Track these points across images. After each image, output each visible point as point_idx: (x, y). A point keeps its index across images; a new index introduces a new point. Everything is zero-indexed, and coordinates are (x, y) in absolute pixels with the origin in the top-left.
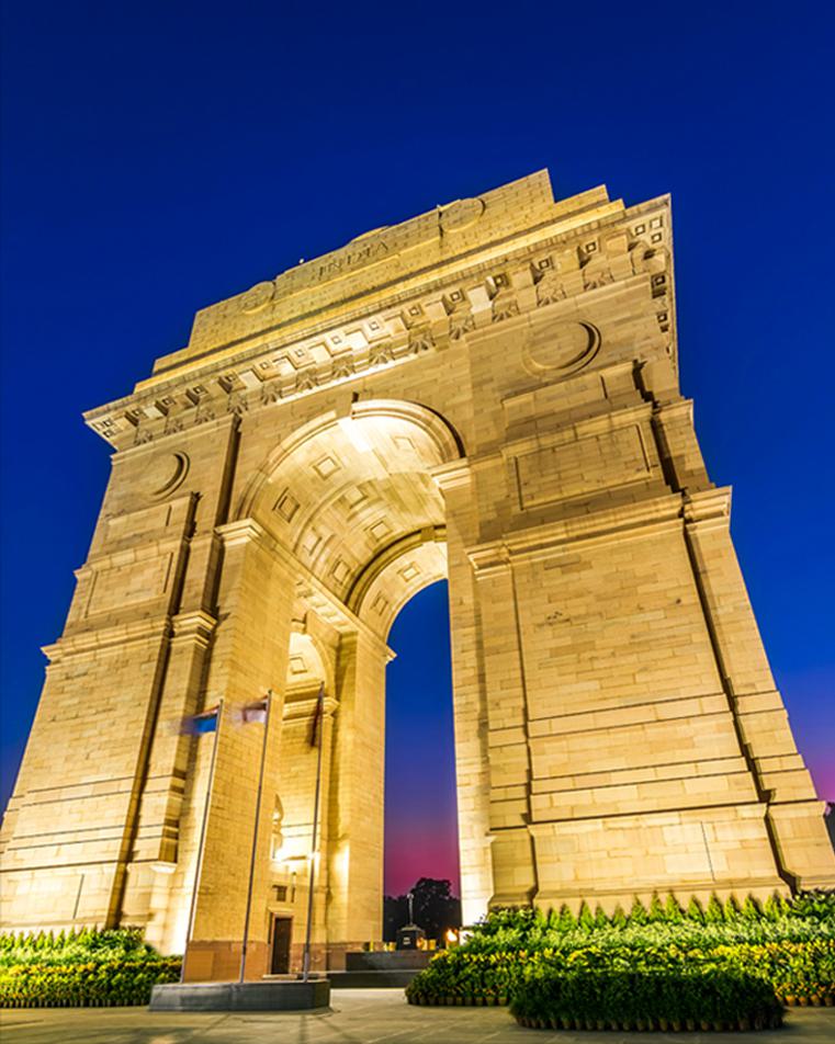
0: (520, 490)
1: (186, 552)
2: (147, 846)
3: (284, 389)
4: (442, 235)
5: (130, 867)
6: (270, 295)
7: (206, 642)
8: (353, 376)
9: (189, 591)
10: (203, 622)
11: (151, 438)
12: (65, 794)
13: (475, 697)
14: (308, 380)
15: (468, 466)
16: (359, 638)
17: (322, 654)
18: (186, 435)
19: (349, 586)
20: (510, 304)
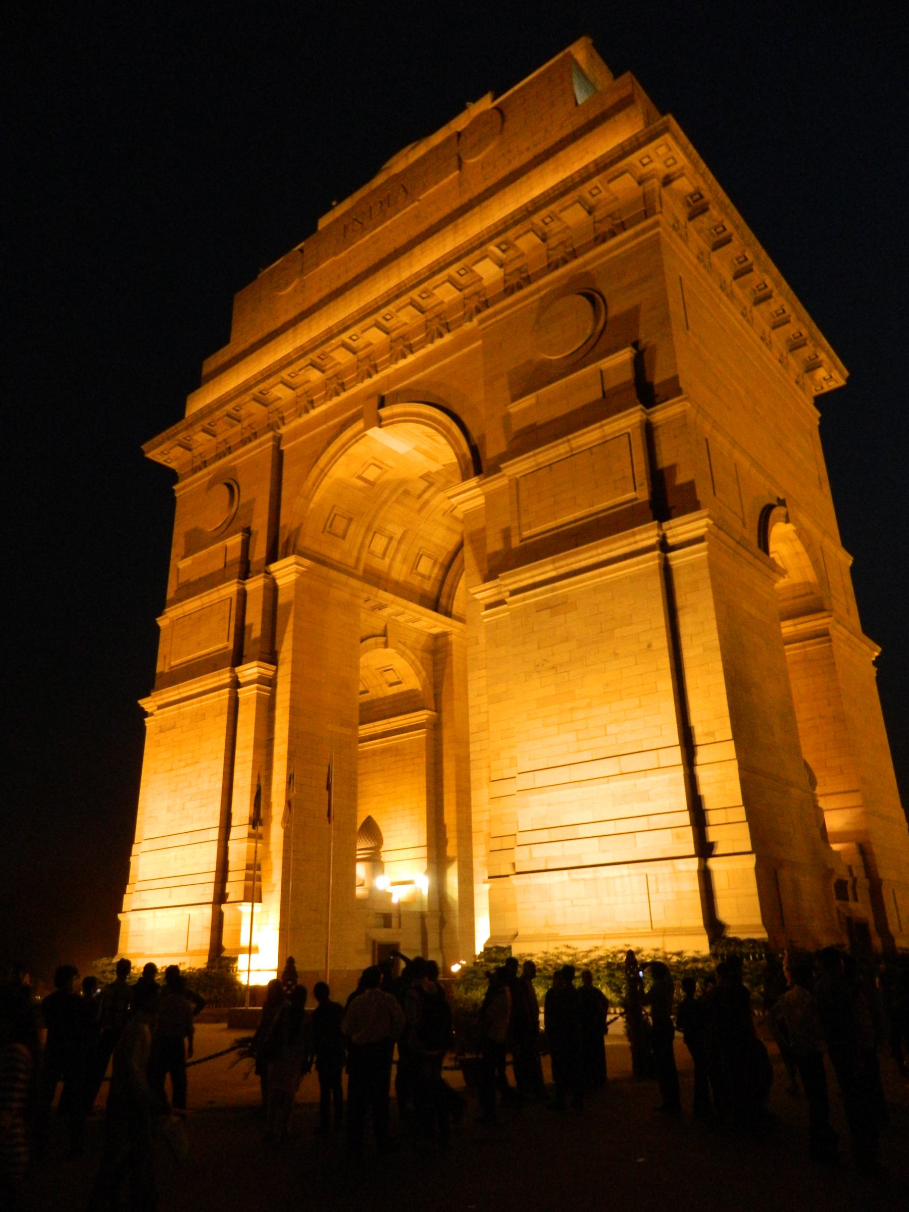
0: (519, 518)
1: (243, 595)
2: (234, 889)
3: (315, 398)
4: (460, 167)
7: (269, 688)
8: (376, 377)
10: (262, 670)
11: (205, 464)
15: (479, 486)
16: (453, 638)
17: (412, 664)
18: (235, 459)
19: (440, 578)
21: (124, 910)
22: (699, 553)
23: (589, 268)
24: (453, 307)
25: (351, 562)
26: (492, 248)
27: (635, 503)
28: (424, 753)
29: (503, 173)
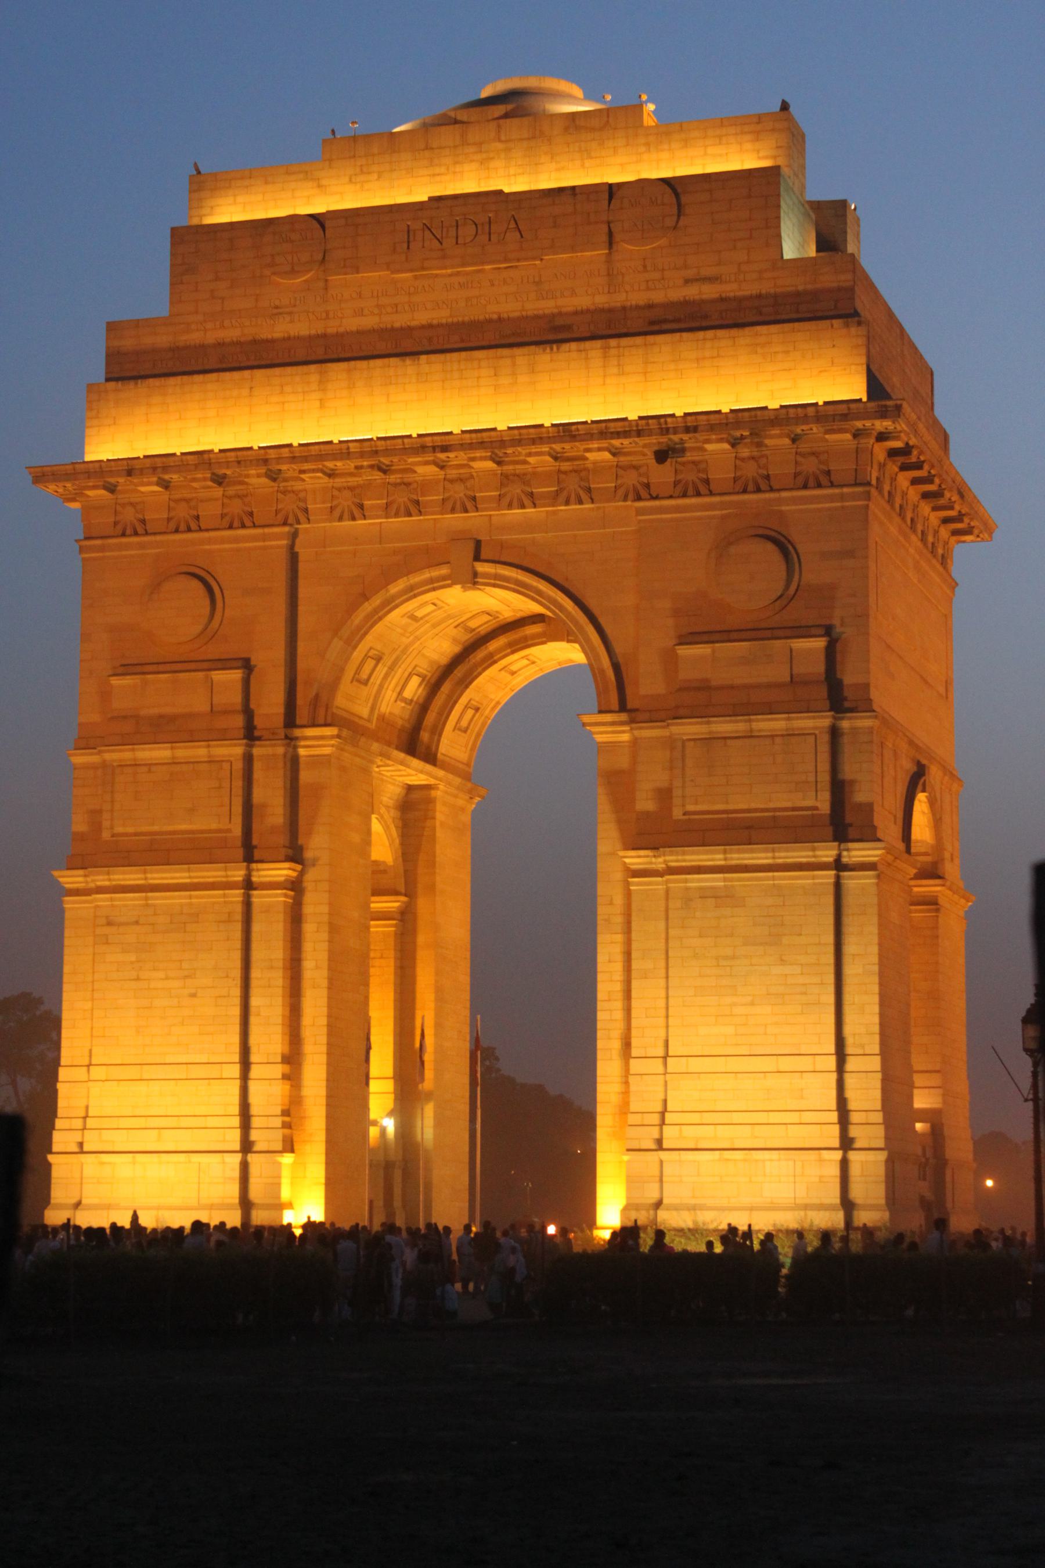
2: (266, 1133)
4: (610, 244)
5: (250, 1157)
6: (320, 257)
7: (292, 893)
12: (148, 1072)
13: (619, 1015)
14: (406, 499)
18: (210, 541)
21: (55, 1149)
23: (783, 508)
24: (599, 468)
25: (365, 712)
27: (815, 812)
28: (391, 954)
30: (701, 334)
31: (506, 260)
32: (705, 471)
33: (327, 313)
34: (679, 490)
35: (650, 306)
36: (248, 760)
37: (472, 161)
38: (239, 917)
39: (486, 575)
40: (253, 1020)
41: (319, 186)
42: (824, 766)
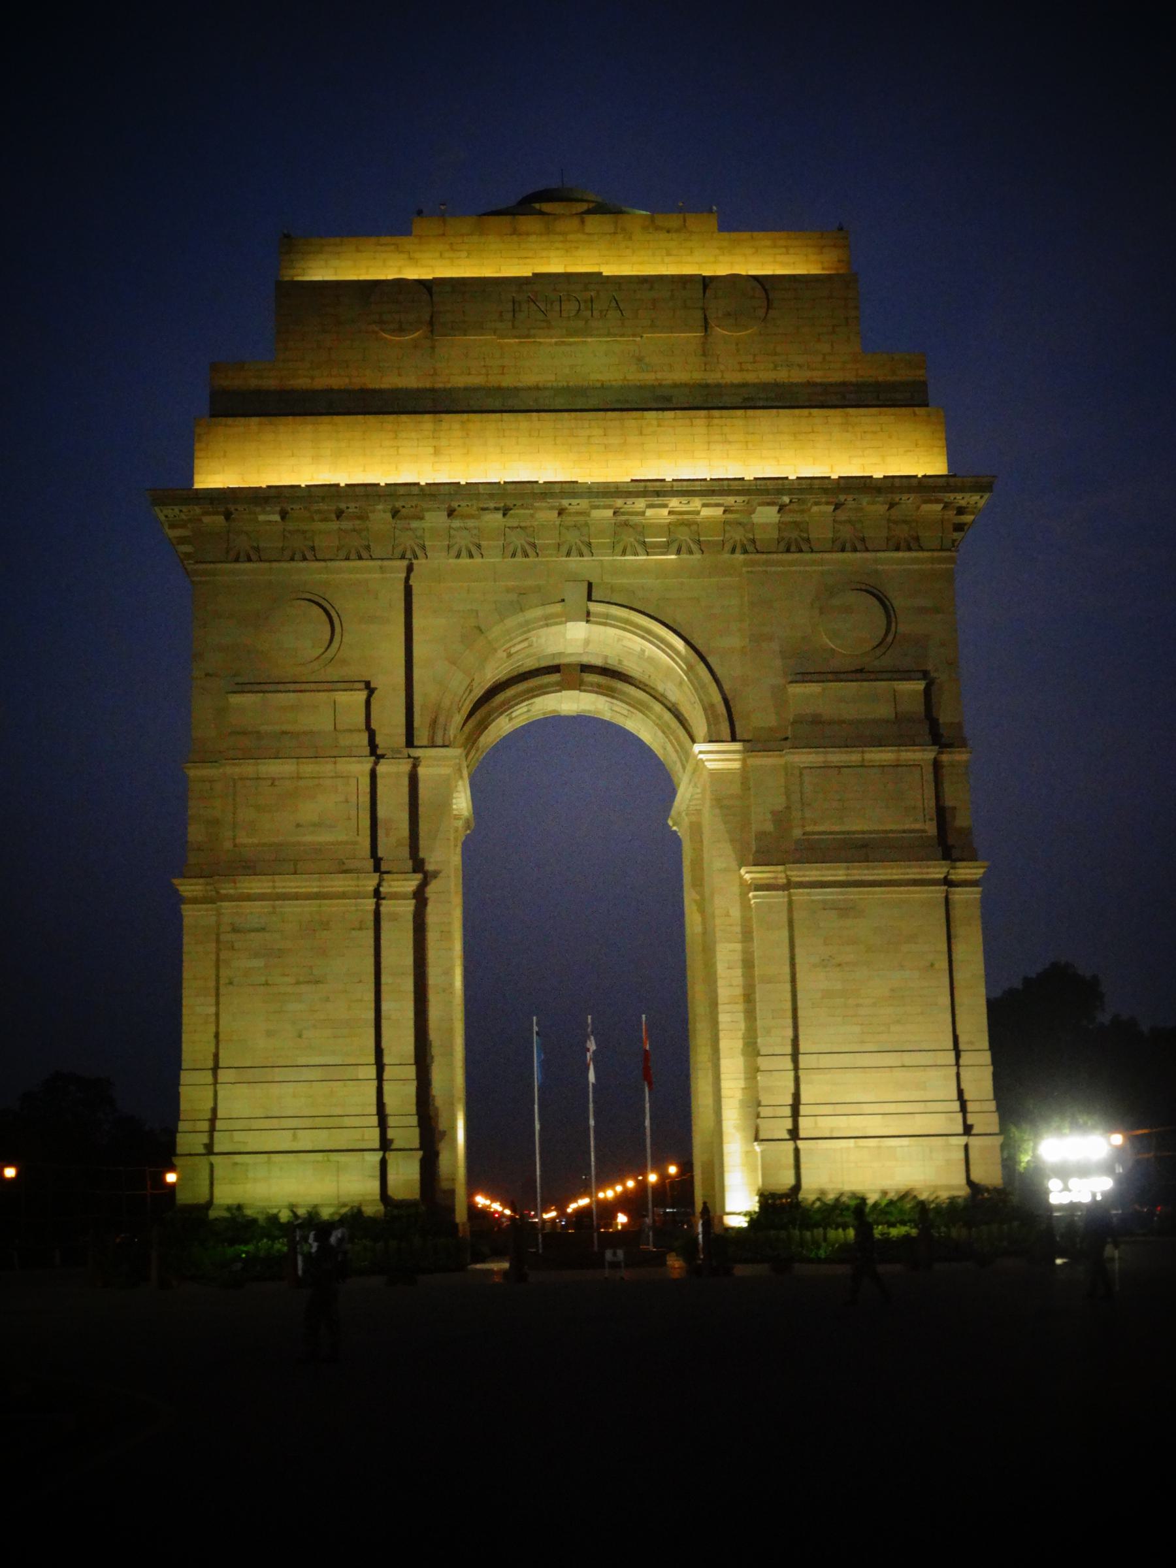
4: (706, 327)
9: (387, 835)
12: (279, 1074)
20: (796, 524)
21: (179, 1150)
22: (974, 894)
26: (786, 499)
29: (764, 374)
30: (797, 411)
31: (609, 335)
32: (807, 531)
33: (435, 369)
34: (782, 546)
35: (744, 385)
36: (373, 775)
37: (557, 249)
38: (371, 924)
39: (599, 615)
40: (385, 1024)
41: (410, 258)
42: (930, 791)
